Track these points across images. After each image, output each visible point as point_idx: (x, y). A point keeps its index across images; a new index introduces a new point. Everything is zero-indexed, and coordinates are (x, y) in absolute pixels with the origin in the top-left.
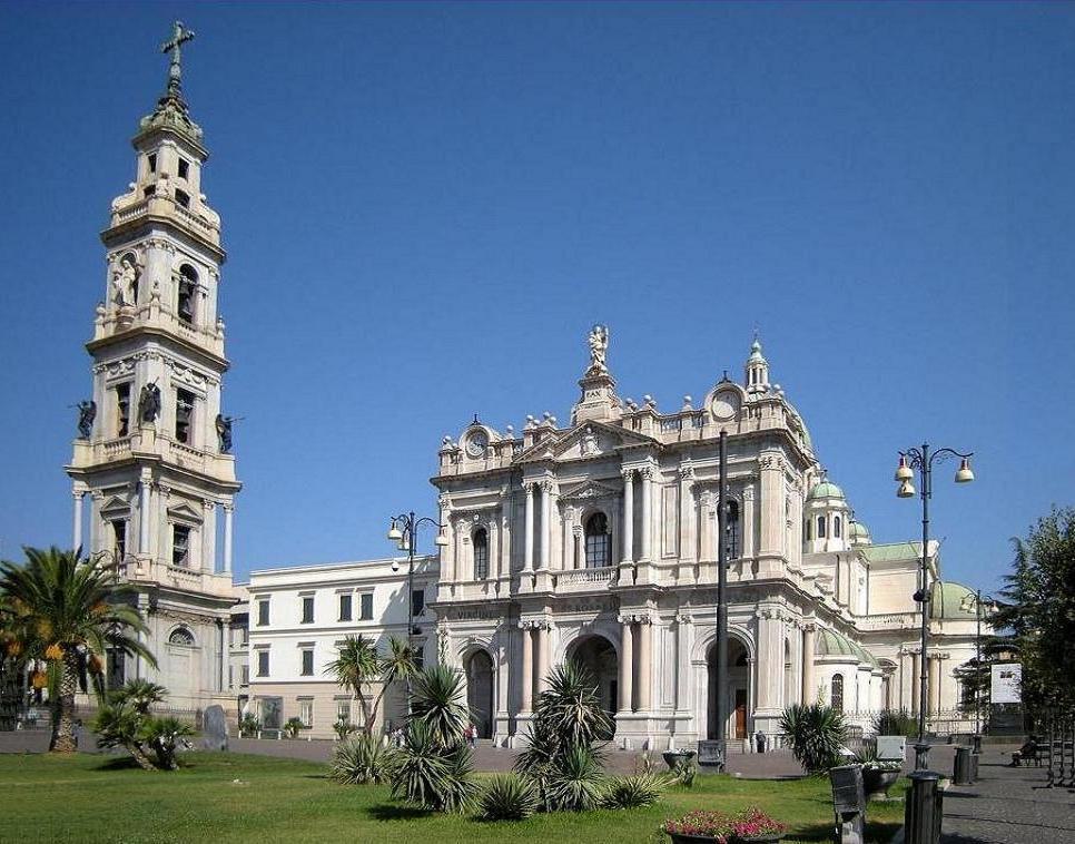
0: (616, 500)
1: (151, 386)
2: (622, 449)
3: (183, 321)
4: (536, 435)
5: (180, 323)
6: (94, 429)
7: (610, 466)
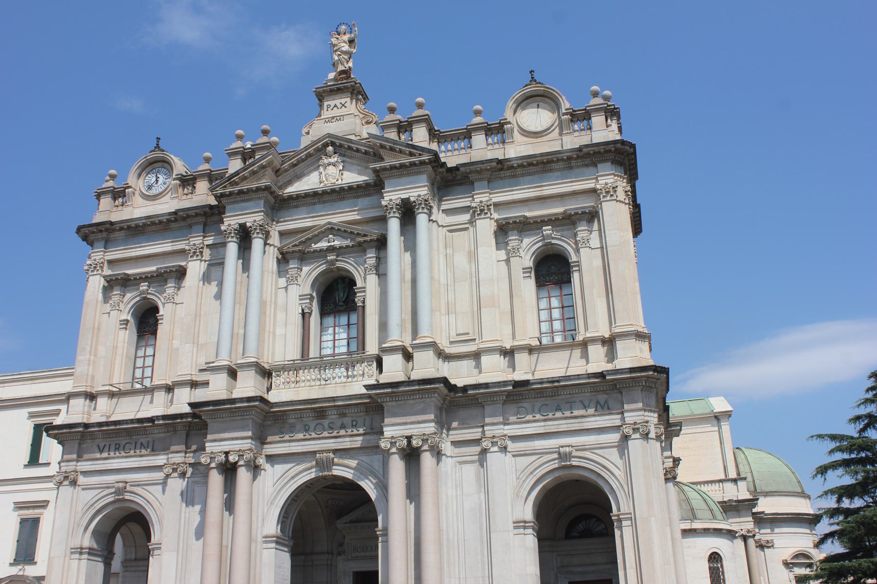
2: (384, 169)
4: (246, 155)
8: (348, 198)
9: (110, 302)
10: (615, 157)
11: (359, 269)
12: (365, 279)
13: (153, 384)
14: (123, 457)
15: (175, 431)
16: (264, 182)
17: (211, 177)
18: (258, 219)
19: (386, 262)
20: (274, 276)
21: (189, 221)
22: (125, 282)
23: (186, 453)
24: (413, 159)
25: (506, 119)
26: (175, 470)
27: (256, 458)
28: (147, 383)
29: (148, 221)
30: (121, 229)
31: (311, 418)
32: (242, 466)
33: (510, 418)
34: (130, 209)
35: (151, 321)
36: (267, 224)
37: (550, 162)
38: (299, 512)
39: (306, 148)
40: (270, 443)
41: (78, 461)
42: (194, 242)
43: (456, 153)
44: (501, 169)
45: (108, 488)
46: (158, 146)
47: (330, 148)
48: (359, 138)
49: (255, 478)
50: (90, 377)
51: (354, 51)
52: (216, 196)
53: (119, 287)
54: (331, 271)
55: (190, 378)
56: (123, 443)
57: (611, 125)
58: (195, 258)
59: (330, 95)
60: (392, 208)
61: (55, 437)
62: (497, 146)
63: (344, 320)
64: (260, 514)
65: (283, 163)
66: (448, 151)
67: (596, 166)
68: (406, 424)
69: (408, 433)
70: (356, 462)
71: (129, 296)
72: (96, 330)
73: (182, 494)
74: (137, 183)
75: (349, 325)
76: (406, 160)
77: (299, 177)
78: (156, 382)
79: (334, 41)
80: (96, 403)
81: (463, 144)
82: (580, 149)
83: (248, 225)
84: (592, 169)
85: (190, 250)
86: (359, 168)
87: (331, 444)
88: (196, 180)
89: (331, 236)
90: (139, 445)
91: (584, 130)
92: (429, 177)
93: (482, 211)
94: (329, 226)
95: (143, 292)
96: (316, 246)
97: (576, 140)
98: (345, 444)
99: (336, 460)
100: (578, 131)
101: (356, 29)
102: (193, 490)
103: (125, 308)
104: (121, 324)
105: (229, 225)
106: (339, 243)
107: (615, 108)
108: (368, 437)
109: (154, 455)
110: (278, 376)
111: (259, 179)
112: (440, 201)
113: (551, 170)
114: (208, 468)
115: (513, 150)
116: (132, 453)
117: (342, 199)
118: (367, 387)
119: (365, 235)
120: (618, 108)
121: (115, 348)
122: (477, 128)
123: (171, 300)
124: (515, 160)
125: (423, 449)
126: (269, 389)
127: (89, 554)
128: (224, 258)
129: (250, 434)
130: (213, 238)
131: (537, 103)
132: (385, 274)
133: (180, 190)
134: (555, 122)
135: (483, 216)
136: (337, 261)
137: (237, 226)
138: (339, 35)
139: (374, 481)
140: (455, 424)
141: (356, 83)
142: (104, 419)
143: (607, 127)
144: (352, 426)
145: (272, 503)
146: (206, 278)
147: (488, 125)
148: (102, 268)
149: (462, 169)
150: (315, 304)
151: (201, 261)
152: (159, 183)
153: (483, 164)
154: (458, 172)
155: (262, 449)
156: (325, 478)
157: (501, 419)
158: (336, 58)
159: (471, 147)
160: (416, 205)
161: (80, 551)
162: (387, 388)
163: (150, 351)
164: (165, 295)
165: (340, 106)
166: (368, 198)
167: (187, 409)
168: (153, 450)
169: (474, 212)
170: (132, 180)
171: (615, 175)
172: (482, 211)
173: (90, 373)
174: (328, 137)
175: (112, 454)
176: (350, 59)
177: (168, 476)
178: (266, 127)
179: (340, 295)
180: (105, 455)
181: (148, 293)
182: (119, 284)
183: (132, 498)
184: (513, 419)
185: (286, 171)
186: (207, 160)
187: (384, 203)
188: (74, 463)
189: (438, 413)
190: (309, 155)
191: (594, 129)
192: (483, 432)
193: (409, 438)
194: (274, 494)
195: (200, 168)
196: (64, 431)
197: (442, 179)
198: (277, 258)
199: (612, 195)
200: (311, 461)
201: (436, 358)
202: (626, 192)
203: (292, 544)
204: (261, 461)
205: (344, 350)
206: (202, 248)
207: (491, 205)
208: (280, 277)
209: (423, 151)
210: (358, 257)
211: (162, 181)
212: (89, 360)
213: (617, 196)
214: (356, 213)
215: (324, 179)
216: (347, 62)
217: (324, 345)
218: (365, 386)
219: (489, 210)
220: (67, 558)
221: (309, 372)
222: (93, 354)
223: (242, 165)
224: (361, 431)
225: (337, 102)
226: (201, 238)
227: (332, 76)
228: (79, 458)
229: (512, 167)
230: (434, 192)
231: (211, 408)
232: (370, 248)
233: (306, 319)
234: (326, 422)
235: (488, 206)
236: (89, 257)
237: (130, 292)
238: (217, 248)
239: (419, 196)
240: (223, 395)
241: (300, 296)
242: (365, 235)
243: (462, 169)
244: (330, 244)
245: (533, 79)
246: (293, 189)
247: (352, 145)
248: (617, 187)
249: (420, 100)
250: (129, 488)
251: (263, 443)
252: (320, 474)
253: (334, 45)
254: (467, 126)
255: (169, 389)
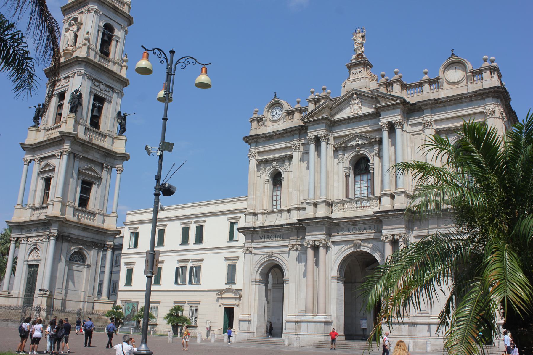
0: (376, 147)
1: (77, 91)
2: (380, 107)
3: (103, 55)
4: (316, 101)
5: (100, 56)
6: (42, 121)
7: (372, 121)
8: (365, 120)
9: (260, 171)
10: (494, 94)
11: (371, 154)
12: (373, 159)
13: (281, 209)
14: (270, 241)
15: (292, 230)
16: (325, 115)
17: (301, 111)
18: (323, 133)
19: (382, 151)
20: (332, 158)
21: (292, 133)
22: (266, 162)
23: (297, 240)
24: (393, 102)
25: (439, 77)
26: (293, 247)
27: (327, 243)
28: (278, 207)
29: (274, 134)
30: (263, 137)
31: (351, 225)
32: (321, 247)
33: (441, 226)
34: (265, 127)
35: (279, 179)
36: (328, 135)
37: (461, 98)
38: (348, 264)
39: (344, 96)
40: (333, 236)
41: (252, 243)
42: (295, 143)
43: (415, 95)
44: (437, 103)
45: (265, 254)
46: (275, 97)
47: (355, 96)
48: (368, 89)
49: (327, 252)
50: (254, 206)
51: (364, 42)
52: (303, 123)
53: (263, 165)
54: (358, 155)
55: (297, 207)
56: (270, 235)
57: (493, 77)
58: (296, 151)
59: (354, 67)
60: (384, 126)
61: (241, 232)
62: (435, 90)
63: (365, 177)
64: (330, 267)
65: (333, 104)
66: (412, 94)
67: (485, 99)
68: (392, 229)
69: (393, 233)
70: (371, 245)
71: (268, 168)
72: (255, 184)
73: (296, 258)
74: (268, 115)
75: (367, 180)
76: (390, 103)
77: (341, 110)
78: (283, 208)
79: (354, 38)
80: (257, 217)
81: (418, 90)
82: (476, 92)
83: (319, 136)
84: (482, 101)
85: (293, 147)
86: (369, 104)
87: (360, 237)
88: (294, 112)
89: (357, 139)
90: (277, 236)
91: (479, 80)
92: (402, 110)
93: (428, 125)
94: (356, 134)
95: (274, 167)
96: (350, 144)
97: (475, 86)
98: (366, 237)
99: (362, 244)
100: (476, 80)
101: (365, 30)
102: (301, 256)
103: (267, 174)
104: (266, 182)
105: (310, 136)
106: (361, 142)
107: (496, 67)
108: (376, 234)
109: (283, 241)
110: (336, 206)
111: (323, 113)
112: (408, 120)
113: (462, 103)
114: (306, 248)
115: (443, 93)
116: (274, 239)
117: (362, 120)
118: (375, 212)
119: (373, 139)
120: (498, 67)
121: (264, 192)
122: (425, 82)
123: (287, 170)
124: (444, 99)
125: (400, 240)
126: (332, 212)
127: (259, 282)
128: (309, 150)
129: (324, 233)
130: (304, 140)
131: (455, 67)
132: (382, 157)
133: (287, 117)
134: (464, 77)
135: (428, 127)
136: (360, 150)
137: (314, 137)
138: (357, 33)
139: (379, 254)
140: (415, 228)
141: (366, 61)
142: (261, 225)
143: (492, 78)
144: (369, 229)
145: (335, 263)
146: (302, 160)
147: (431, 80)
148: (255, 156)
149: (418, 104)
150: (351, 171)
151: (299, 152)
152: (277, 114)
153: (428, 101)
154: (416, 106)
155: (330, 239)
156: (358, 251)
157: (436, 226)
158: (356, 47)
159: (422, 91)
160: (395, 125)
161: (255, 281)
162: (383, 213)
163: (279, 193)
164: (284, 168)
165: (359, 72)
166: (373, 120)
167: (297, 221)
168: (283, 238)
169: (424, 125)
170: (265, 114)
171: (494, 104)
172: (428, 125)
173: (254, 204)
174: (353, 90)
175: (266, 240)
176: (362, 46)
177: (290, 250)
178: (324, 87)
179: (363, 166)
180: (263, 240)
181: (276, 167)
182: (263, 163)
183: (275, 259)
184: (442, 226)
185: (335, 108)
186: (298, 102)
187: (380, 124)
188: (250, 244)
189: (407, 223)
190: (345, 100)
191: (484, 80)
192: (428, 232)
193: (393, 235)
194: (336, 259)
195: (295, 107)
196: (245, 230)
197: (408, 109)
198: (333, 150)
199: (492, 115)
200: (351, 244)
201: (406, 198)
202: (500, 112)
203: (344, 280)
204: (329, 244)
205: (366, 191)
206: (299, 146)
207: (432, 122)
208: (335, 159)
209: (399, 98)
210: (370, 148)
211: (279, 114)
212: (253, 198)
213: (495, 115)
214: (368, 127)
215: (353, 111)
216: (361, 48)
217: (356, 189)
218: (373, 212)
219: (431, 124)
220: (250, 284)
221: (349, 204)
222: (254, 195)
223: (315, 108)
224: (373, 231)
225: (357, 70)
226: (298, 141)
227: (354, 56)
228: (252, 241)
229: (442, 102)
230: (404, 116)
231: (307, 221)
232: (376, 144)
233: (348, 178)
234: (357, 227)
235: (431, 122)
236: (249, 151)
237: (268, 166)
238: (306, 145)
239: (397, 120)
240: (312, 216)
241: (344, 168)
242: (373, 139)
243: (418, 104)
244: (357, 143)
245: (453, 54)
246: (338, 117)
247: (365, 94)
248: (495, 110)
249: (396, 70)
250: (274, 255)
251: (330, 236)
252: (355, 250)
253: (355, 40)
254: (420, 81)
255: (288, 211)
